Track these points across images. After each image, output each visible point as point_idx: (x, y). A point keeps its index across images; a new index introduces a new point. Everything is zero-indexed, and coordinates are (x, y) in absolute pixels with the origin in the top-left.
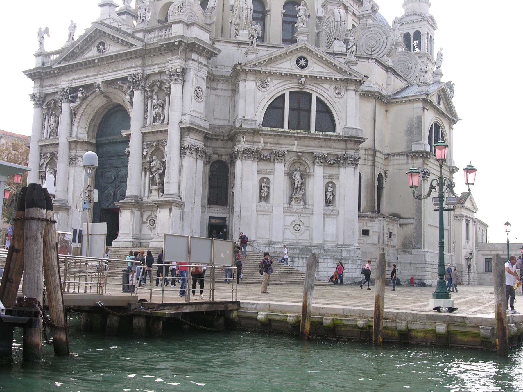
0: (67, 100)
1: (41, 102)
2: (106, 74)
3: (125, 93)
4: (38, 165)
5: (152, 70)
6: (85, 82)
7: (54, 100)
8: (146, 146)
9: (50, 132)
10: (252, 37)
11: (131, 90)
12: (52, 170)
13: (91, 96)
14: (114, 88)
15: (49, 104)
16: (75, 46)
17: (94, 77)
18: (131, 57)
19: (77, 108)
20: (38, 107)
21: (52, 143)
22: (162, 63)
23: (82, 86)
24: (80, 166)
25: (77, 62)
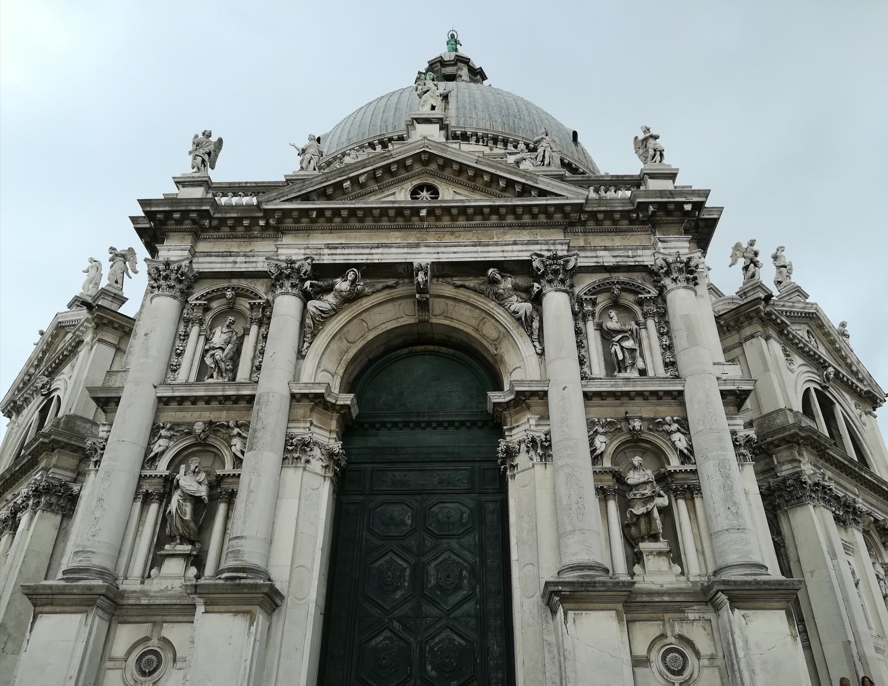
0: (296, 291)
2: (446, 246)
3: (500, 299)
5: (595, 260)
6: (370, 257)
7: (233, 289)
8: (601, 430)
10: (752, 265)
12: (202, 476)
13: (373, 297)
14: (462, 286)
15: (210, 297)
16: (351, 175)
17: (405, 250)
19: (326, 316)
20: (175, 297)
21: (220, 393)
22: (625, 249)
24: (316, 473)
25: (357, 206)
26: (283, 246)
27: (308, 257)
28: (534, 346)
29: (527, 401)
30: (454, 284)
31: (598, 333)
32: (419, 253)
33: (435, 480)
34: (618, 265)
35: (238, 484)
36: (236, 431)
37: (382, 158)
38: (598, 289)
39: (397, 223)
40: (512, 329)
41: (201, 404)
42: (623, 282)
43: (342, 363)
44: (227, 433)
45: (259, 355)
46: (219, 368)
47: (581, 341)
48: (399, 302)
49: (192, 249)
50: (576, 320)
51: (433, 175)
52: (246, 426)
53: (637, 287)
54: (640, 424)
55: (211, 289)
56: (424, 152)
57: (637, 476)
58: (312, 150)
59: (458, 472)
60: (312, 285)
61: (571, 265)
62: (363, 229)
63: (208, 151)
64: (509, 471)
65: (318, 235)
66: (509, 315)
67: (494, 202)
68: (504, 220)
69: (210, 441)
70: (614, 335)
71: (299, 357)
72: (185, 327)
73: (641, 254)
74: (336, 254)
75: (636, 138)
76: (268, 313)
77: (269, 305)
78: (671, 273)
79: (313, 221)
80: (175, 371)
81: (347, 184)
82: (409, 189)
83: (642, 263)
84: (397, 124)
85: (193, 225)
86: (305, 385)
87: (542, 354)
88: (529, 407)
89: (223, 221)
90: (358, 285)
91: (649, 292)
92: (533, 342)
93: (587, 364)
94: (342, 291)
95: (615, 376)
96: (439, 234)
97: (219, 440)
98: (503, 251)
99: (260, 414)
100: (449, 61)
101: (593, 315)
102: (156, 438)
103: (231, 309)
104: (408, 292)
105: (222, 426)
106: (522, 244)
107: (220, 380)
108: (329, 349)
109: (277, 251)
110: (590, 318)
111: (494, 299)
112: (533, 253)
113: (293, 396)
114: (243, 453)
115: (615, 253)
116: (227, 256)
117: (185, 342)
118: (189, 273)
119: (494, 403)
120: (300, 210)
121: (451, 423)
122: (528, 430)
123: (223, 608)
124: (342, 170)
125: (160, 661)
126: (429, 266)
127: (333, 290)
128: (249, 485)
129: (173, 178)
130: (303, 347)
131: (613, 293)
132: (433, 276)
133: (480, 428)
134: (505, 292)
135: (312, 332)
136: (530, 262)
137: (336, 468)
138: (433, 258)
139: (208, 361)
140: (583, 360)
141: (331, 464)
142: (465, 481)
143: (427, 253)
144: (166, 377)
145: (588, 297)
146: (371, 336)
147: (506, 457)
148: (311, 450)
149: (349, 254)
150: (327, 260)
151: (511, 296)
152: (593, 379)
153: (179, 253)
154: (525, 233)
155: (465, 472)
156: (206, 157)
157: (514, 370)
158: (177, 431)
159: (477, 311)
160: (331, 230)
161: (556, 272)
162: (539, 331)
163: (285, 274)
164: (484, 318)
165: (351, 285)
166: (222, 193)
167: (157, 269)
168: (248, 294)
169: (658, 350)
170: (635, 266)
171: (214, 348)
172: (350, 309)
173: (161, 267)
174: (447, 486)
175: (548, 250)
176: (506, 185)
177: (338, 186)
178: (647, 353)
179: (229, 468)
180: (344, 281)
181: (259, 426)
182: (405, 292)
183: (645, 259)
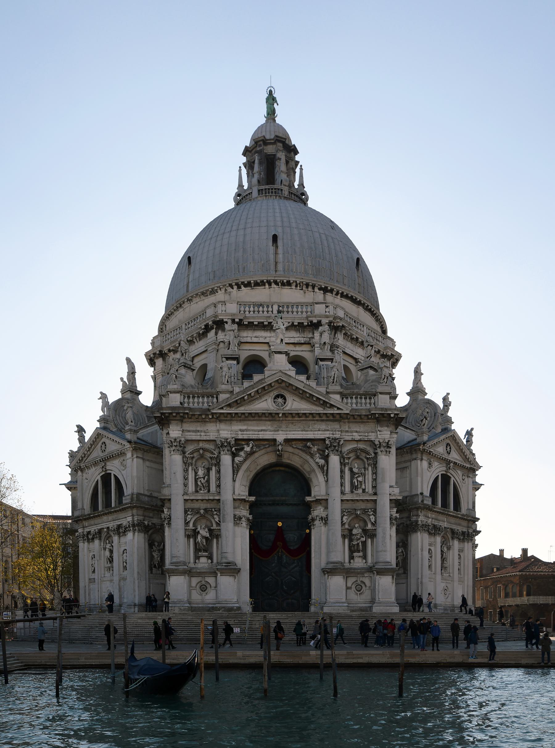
3: (312, 456)
4: (184, 520)
6: (258, 436)
11: (326, 454)
13: (259, 452)
17: (273, 433)
19: (242, 463)
24: (244, 527)
30: (293, 447)
36: (215, 513)
41: (200, 501)
51: (283, 388)
52: (219, 510)
69: (206, 516)
79: (232, 417)
100: (270, 140)
103: (202, 457)
113: (234, 499)
114: (220, 521)
123: (226, 574)
125: (207, 588)
139: (199, 483)
146: (258, 468)
161: (335, 446)
171: (200, 478)
179: (214, 527)
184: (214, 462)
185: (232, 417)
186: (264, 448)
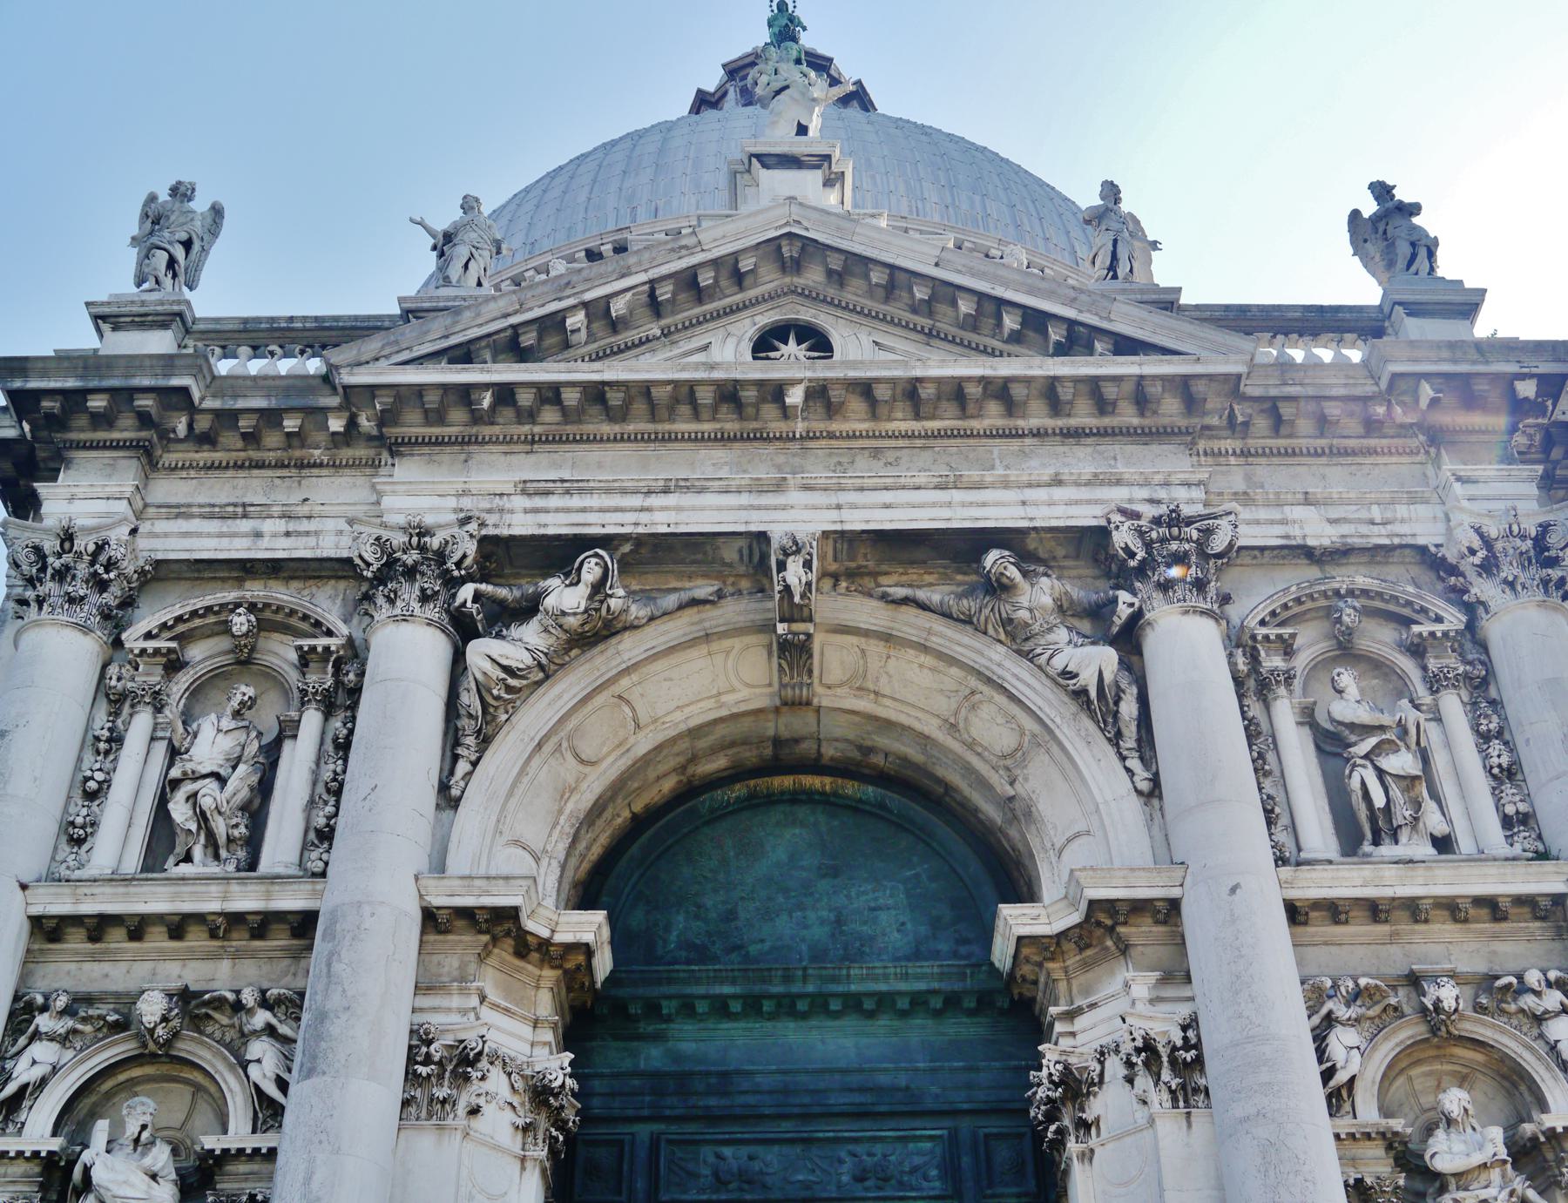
0: (433, 611)
1: (110, 598)
2: (862, 489)
3: (1018, 637)
5: (1279, 530)
6: (644, 517)
7: (252, 608)
9: (162, 831)
11: (1124, 612)
13: (650, 630)
14: (906, 601)
15: (183, 631)
16: (588, 296)
17: (745, 499)
18: (1107, 421)
20: (85, 629)
22: (1359, 502)
23: (606, 541)
26: (397, 487)
27: (470, 518)
28: (1128, 770)
29: (1121, 929)
30: (884, 597)
31: (1306, 731)
32: (784, 508)
33: (845, 1168)
34: (1344, 544)
35: (270, 1178)
36: (262, 1018)
37: (673, 250)
38: (1297, 609)
39: (718, 426)
40: (1058, 720)
42: (1365, 593)
43: (562, 821)
44: (233, 1026)
45: (325, 797)
46: (211, 838)
47: (1261, 756)
48: (727, 643)
49: (138, 497)
50: (1241, 696)
52: (292, 1005)
53: (1404, 606)
54: (1456, 991)
55: (189, 609)
56: (790, 235)
57: (1458, 1147)
58: (473, 235)
59: (911, 1146)
60: (477, 597)
61: (1218, 543)
62: (622, 439)
63: (184, 236)
64: (1073, 1138)
65: (493, 457)
66: (1048, 682)
67: (995, 370)
68: (1023, 417)
69: (185, 1048)
70: (1353, 738)
71: (443, 804)
72: (110, 714)
73: (1406, 515)
74: (546, 511)
75: (1355, 215)
76: (351, 676)
77: (355, 653)
78: (1498, 567)
79: (477, 418)
80: (79, 842)
81: (576, 320)
82: (749, 335)
83: (1410, 541)
84: (661, 204)
85: (140, 430)
86: (466, 882)
87: (1153, 792)
88: (1124, 949)
89: (227, 418)
90: (611, 596)
91: (1439, 619)
92: (1123, 758)
93: (1284, 820)
94: (564, 613)
95: (1369, 855)
96: (841, 455)
97: (210, 1047)
98: (1024, 503)
99: (337, 967)
101: (1289, 679)
102: (22, 1041)
103: (244, 660)
104: (751, 617)
105: (218, 1004)
106: (1077, 484)
107: (214, 869)
108: (525, 780)
109: (378, 503)
110: (1282, 691)
111: (1002, 637)
112: (1113, 506)
114: (283, 1085)
115: (1335, 513)
116: (234, 517)
117: (112, 757)
118: (125, 564)
119: (1020, 939)
120: (445, 388)
121: (885, 1002)
122: (1132, 1014)
124: (565, 281)
126: (815, 544)
127: (538, 610)
128: (308, 1180)
129: (88, 304)
130: (452, 773)
131: (1339, 620)
132: (824, 574)
133: (971, 1013)
134: (1034, 618)
135: (479, 732)
136: (1101, 534)
137: (554, 1133)
138: (827, 521)
139: (179, 810)
140: (1272, 811)
141: (543, 1123)
142: (934, 1173)
143: (806, 507)
144: (53, 858)
145: (1272, 632)
146: (643, 744)
147: (1063, 1099)
148: (483, 1078)
149: (584, 510)
150: (521, 525)
151: (1050, 630)
152: (1308, 863)
153: (101, 506)
154: (1081, 455)
155: (929, 1145)
156: (179, 253)
157: (1069, 841)
158: (84, 1020)
159: (954, 671)
160: (533, 442)
162: (1138, 726)
163: (404, 565)
164: (973, 693)
165: (591, 598)
166: (223, 347)
167: (37, 550)
168: (294, 621)
169: (1480, 785)
170: (1388, 550)
172: (587, 666)
173: (50, 545)
174: (880, 1188)
175: (1151, 501)
176: (1021, 324)
177: (553, 324)
178: (1448, 789)
179: (239, 1134)
180: (571, 584)
181: (335, 1002)
182: (742, 618)
183: (1418, 528)
184: (321, 679)
185: (477, 418)
186: (681, 607)
